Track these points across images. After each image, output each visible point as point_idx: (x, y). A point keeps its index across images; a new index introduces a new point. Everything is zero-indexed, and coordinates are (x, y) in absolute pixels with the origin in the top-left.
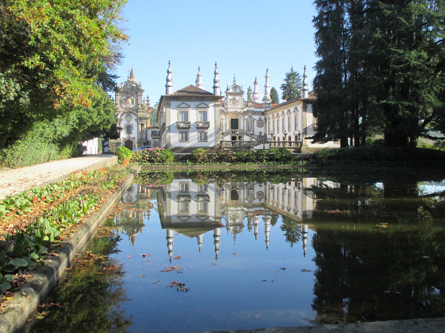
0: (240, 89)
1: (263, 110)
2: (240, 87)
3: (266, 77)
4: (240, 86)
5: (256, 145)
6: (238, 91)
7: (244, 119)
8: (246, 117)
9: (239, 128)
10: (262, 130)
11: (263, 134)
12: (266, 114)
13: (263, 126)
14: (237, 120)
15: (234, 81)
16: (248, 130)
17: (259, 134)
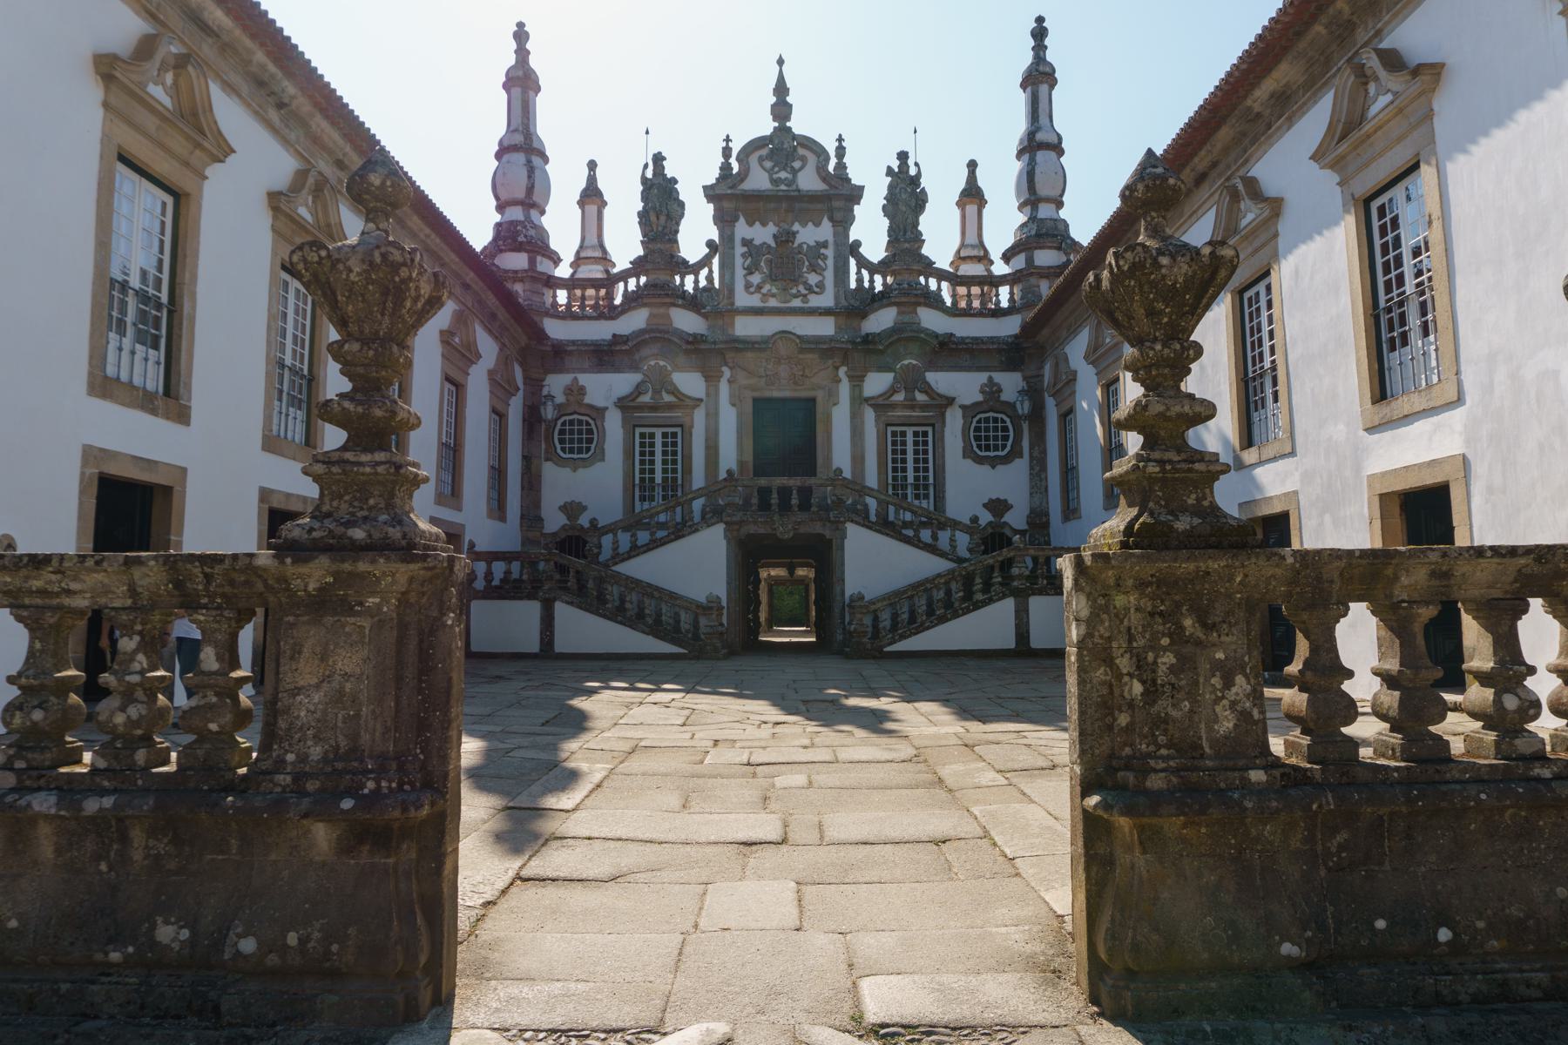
0: (821, 169)
1: (1010, 327)
2: (820, 152)
3: (1039, 78)
4: (831, 150)
5: (947, 610)
6: (808, 181)
7: (858, 400)
8: (877, 383)
9: (818, 470)
10: (1011, 482)
11: (1016, 518)
12: (1041, 353)
13: (1016, 453)
14: (812, 401)
15: (782, 110)
16: (900, 485)
17: (986, 517)
